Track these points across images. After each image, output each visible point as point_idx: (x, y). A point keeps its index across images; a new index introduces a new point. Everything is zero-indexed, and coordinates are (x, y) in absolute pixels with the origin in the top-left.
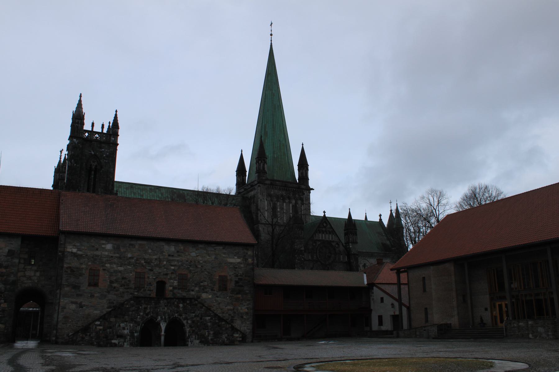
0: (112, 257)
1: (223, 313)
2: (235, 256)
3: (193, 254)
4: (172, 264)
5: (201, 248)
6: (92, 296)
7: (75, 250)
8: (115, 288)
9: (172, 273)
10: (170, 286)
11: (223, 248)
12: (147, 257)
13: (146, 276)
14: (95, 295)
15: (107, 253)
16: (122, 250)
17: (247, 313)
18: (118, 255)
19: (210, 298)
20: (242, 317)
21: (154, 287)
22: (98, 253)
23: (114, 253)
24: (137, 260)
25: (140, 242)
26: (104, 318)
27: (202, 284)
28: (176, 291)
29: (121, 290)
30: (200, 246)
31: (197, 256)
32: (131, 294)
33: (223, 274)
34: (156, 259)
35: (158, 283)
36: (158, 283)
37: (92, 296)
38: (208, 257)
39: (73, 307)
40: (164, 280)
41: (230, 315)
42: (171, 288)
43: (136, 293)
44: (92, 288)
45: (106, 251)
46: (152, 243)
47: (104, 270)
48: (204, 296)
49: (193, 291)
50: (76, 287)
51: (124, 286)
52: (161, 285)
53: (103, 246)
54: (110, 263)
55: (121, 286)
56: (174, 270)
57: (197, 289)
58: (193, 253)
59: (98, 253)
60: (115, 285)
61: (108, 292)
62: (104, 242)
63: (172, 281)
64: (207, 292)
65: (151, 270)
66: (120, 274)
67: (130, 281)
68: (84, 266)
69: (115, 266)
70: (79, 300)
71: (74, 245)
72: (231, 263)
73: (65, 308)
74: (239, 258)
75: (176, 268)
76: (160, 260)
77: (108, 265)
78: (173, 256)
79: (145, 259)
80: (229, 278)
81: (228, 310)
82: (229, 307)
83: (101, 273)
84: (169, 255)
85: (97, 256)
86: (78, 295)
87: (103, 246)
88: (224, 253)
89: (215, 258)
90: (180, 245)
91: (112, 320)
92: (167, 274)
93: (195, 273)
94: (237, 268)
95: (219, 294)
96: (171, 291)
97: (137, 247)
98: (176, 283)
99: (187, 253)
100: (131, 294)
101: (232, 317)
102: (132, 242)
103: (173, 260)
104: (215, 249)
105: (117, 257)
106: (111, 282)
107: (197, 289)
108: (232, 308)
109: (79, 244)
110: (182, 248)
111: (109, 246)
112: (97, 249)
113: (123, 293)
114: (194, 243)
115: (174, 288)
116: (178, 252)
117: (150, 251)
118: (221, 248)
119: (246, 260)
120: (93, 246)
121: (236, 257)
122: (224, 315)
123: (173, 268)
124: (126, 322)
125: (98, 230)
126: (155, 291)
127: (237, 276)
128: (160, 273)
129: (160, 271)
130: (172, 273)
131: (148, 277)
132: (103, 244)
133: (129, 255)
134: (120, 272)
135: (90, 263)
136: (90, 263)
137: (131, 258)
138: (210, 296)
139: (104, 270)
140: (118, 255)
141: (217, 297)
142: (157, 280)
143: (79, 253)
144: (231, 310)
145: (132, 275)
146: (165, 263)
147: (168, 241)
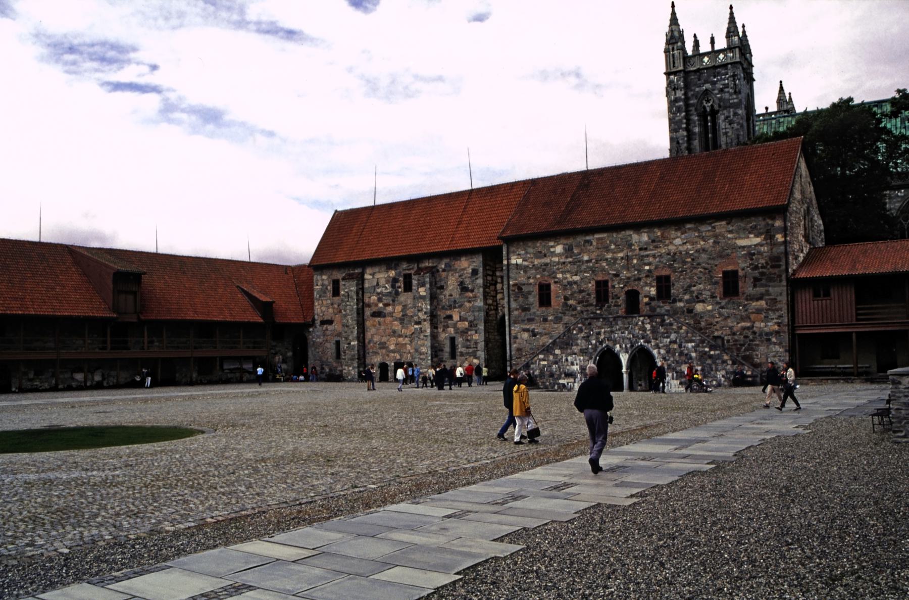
0: (564, 263)
1: (734, 334)
2: (750, 233)
3: (678, 241)
4: (646, 261)
5: (689, 229)
6: (545, 320)
7: (520, 261)
8: (571, 306)
9: (647, 276)
10: (646, 296)
11: (728, 224)
12: (609, 256)
13: (610, 284)
14: (550, 318)
15: (556, 259)
16: (576, 251)
17: (777, 333)
18: (570, 260)
19: (709, 311)
20: (769, 340)
21: (622, 300)
22: (547, 260)
23: (567, 257)
24: (597, 262)
25: (597, 236)
26: (547, 350)
27: (693, 289)
28: (653, 303)
29: (579, 308)
30: (688, 226)
31: (685, 243)
32: (592, 313)
33: (730, 268)
34: (622, 258)
35: (628, 293)
36: (628, 293)
37: (545, 320)
38: (702, 243)
39: (526, 335)
40: (635, 288)
41: (746, 337)
42: (646, 300)
43: (598, 312)
44: (544, 309)
45: (557, 255)
46: (615, 235)
47: (555, 282)
48: (699, 307)
49: (680, 300)
50: (525, 309)
51: (582, 302)
52: (633, 297)
53: (552, 250)
54: (562, 273)
55: (579, 303)
56: (649, 271)
57: (687, 297)
58: (678, 241)
59: (547, 260)
60: (571, 302)
61: (564, 313)
62: (552, 244)
63: (647, 288)
64: (703, 301)
65: (617, 275)
66: (575, 286)
67: (589, 294)
68: (532, 281)
69: (568, 276)
70: (531, 326)
71: (519, 255)
72: (744, 247)
73: (516, 338)
74: (757, 236)
75: (653, 268)
76: (628, 258)
77: (560, 276)
78: (646, 249)
79: (607, 259)
80: (741, 273)
81: (744, 328)
82: (743, 324)
83: (553, 287)
84: (641, 249)
85: (546, 264)
86: (530, 320)
87: (552, 250)
88: (730, 232)
89: (714, 242)
90: (656, 230)
91: (557, 352)
92: (639, 279)
93: (682, 271)
94: (754, 254)
95: (723, 303)
96: (647, 304)
97: (594, 243)
98: (653, 291)
99: (667, 242)
100: (592, 313)
101: (751, 340)
102: (588, 238)
103: (647, 256)
104: (714, 227)
105: (570, 262)
106: (566, 299)
107: (687, 297)
108: (748, 324)
109: (523, 252)
110: (659, 234)
111: (559, 249)
112: (545, 256)
113: (582, 312)
114: (678, 223)
115: (652, 299)
116: (653, 241)
117: (613, 247)
118: (724, 223)
119: (772, 237)
120: (540, 252)
121: (752, 236)
122: (736, 337)
123: (647, 268)
124: (575, 354)
125: (543, 227)
126: (623, 306)
127: (756, 268)
128: (629, 278)
129: (629, 275)
130: (647, 276)
131: (613, 287)
132: (552, 247)
133: (586, 258)
134: (575, 283)
135: (538, 276)
136: (538, 276)
137: (587, 261)
138: (710, 308)
139: (555, 282)
140: (570, 260)
141: (722, 308)
142: (626, 289)
143: (526, 263)
144: (748, 328)
145: (591, 286)
146: (635, 261)
147: (637, 227)
